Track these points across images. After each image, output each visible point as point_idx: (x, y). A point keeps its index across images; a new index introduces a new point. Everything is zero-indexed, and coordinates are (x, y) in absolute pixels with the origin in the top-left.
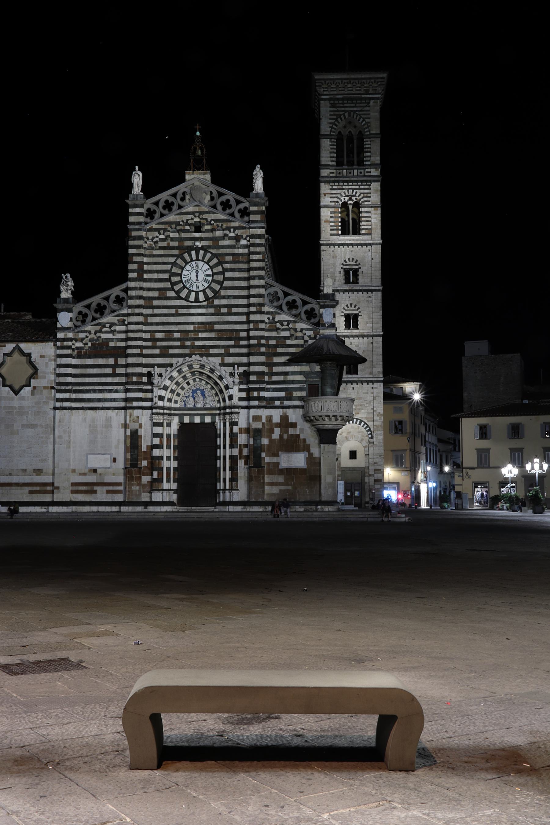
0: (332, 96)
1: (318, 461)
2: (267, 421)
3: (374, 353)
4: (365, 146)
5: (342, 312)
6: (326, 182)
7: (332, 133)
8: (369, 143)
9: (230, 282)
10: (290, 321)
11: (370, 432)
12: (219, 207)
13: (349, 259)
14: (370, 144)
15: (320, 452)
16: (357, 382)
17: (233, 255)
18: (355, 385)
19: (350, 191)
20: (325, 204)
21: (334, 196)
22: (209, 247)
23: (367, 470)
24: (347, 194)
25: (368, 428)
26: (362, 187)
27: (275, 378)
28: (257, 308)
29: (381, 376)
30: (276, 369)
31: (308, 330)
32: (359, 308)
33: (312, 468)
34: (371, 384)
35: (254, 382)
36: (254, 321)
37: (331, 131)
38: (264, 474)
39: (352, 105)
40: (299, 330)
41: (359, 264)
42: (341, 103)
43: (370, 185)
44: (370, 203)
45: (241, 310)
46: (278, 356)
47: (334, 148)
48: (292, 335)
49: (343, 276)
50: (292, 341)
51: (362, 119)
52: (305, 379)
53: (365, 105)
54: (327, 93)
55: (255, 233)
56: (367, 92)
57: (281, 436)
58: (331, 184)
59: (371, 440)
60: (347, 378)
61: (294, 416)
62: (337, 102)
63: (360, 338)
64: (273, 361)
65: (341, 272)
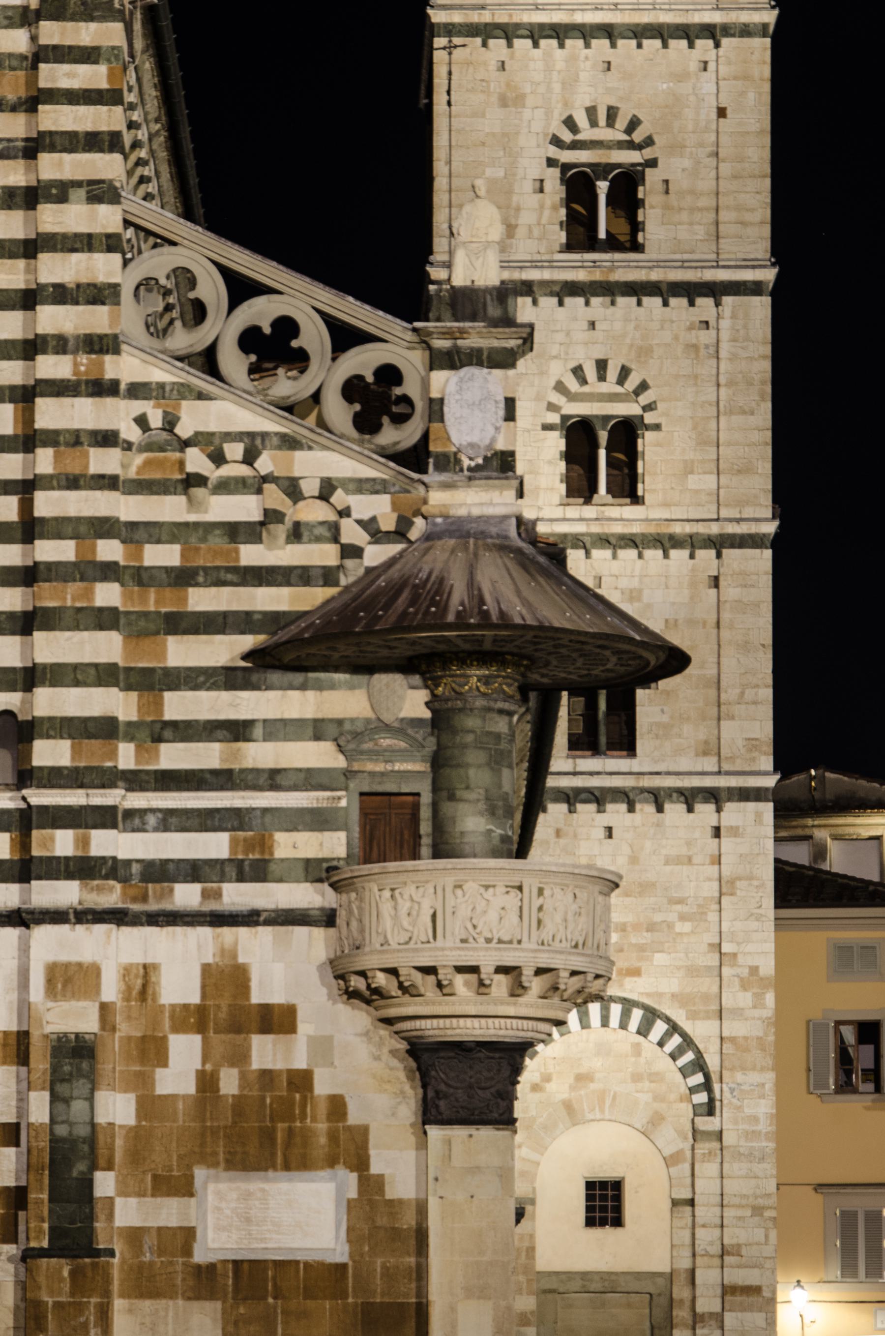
1: (409, 1220)
3: (725, 634)
5: (552, 407)
10: (264, 435)
11: (699, 1079)
15: (422, 1169)
18: (616, 812)
23: (681, 1292)
25: (689, 1056)
29: (767, 763)
31: (362, 486)
32: (643, 387)
33: (379, 1261)
34: (705, 811)
36: (57, 432)
38: (107, 1294)
40: (310, 487)
41: (649, 142)
46: (196, 631)
48: (272, 516)
49: (554, 208)
50: (270, 549)
52: (340, 762)
59: (707, 1124)
64: (163, 655)
65: (547, 186)
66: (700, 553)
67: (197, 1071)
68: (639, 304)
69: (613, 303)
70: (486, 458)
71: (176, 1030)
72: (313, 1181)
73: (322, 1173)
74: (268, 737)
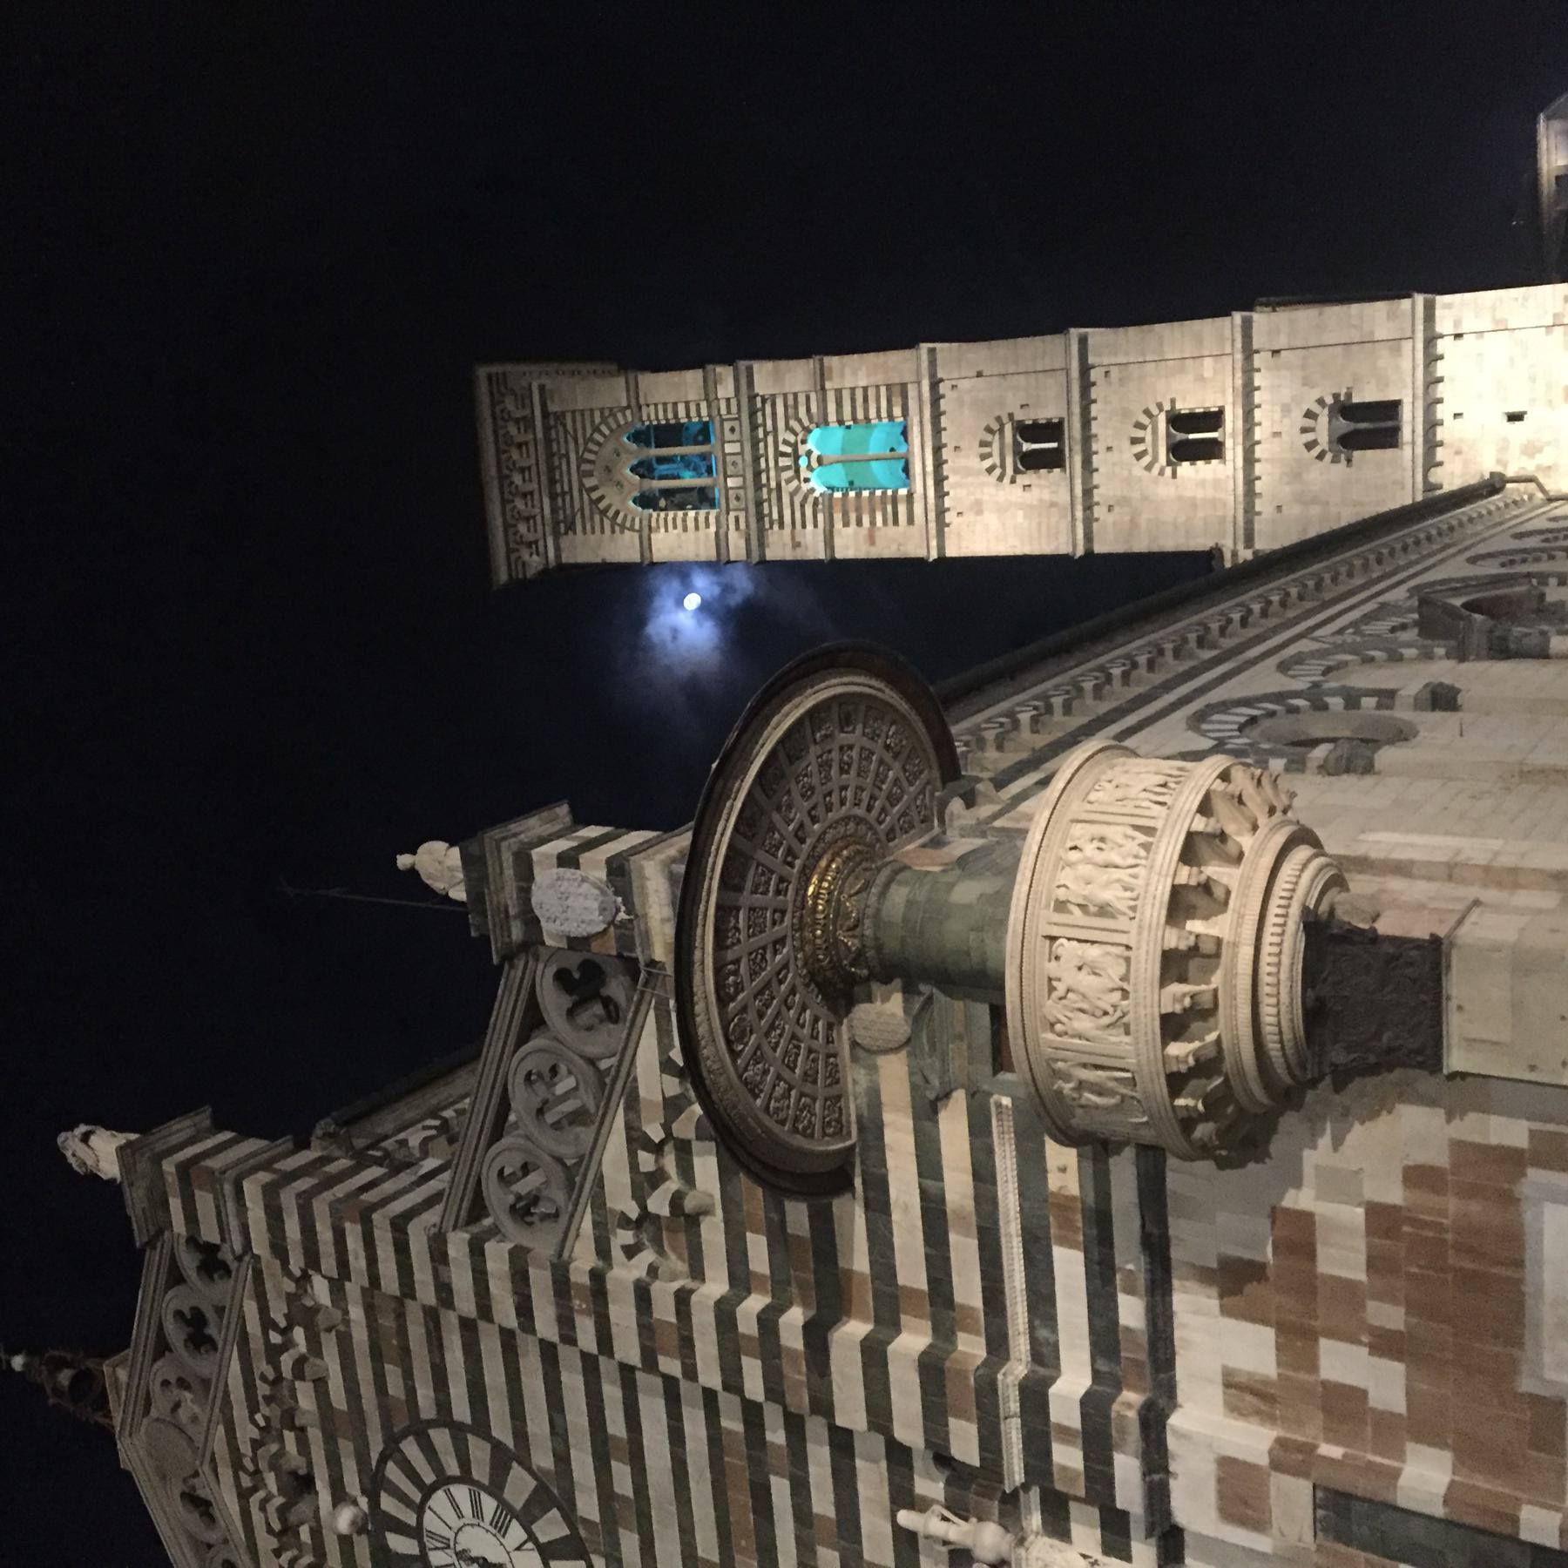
0: (547, 529)
2: (1268, 1418)
4: (663, 422)
5: (1161, 473)
6: (762, 545)
7: (637, 526)
8: (652, 407)
9: (492, 1405)
10: (629, 1127)
12: (204, 1365)
13: (984, 457)
14: (656, 405)
16: (1432, 404)
17: (377, 1356)
18: (1442, 412)
19: (783, 462)
20: (822, 545)
21: (798, 515)
22: (362, 1458)
24: (790, 473)
26: (769, 423)
27: (968, 1289)
28: (582, 1312)
29: (1405, 304)
30: (912, 1272)
32: (1147, 412)
34: (1442, 346)
35: (990, 1441)
37: (632, 529)
39: (564, 467)
41: (998, 419)
42: (564, 501)
43: (764, 401)
44: (813, 397)
45: (612, 1393)
47: (674, 520)
49: (1040, 477)
51: (597, 437)
52: (959, 1097)
53: (561, 429)
54: (541, 543)
55: (266, 1236)
56: (528, 422)
57: (1385, 1344)
58: (767, 526)
60: (1413, 443)
61: (1222, 1218)
62: (561, 512)
63: (1257, 401)
66: (1256, 364)
67: (1370, 1354)
68: (1095, 419)
69: (1096, 436)
70: (616, 893)
71: (1313, 1368)
72: (1540, 1233)
73: (1528, 1216)
74: (939, 1177)
